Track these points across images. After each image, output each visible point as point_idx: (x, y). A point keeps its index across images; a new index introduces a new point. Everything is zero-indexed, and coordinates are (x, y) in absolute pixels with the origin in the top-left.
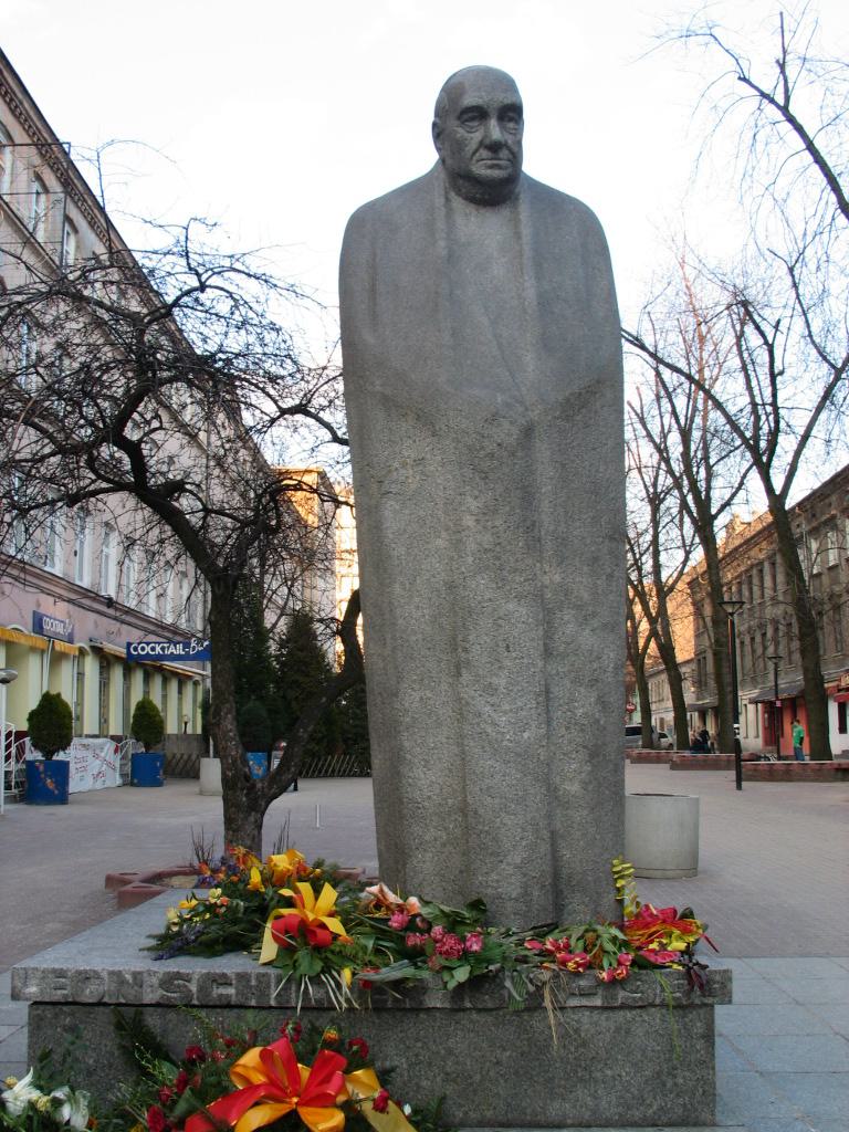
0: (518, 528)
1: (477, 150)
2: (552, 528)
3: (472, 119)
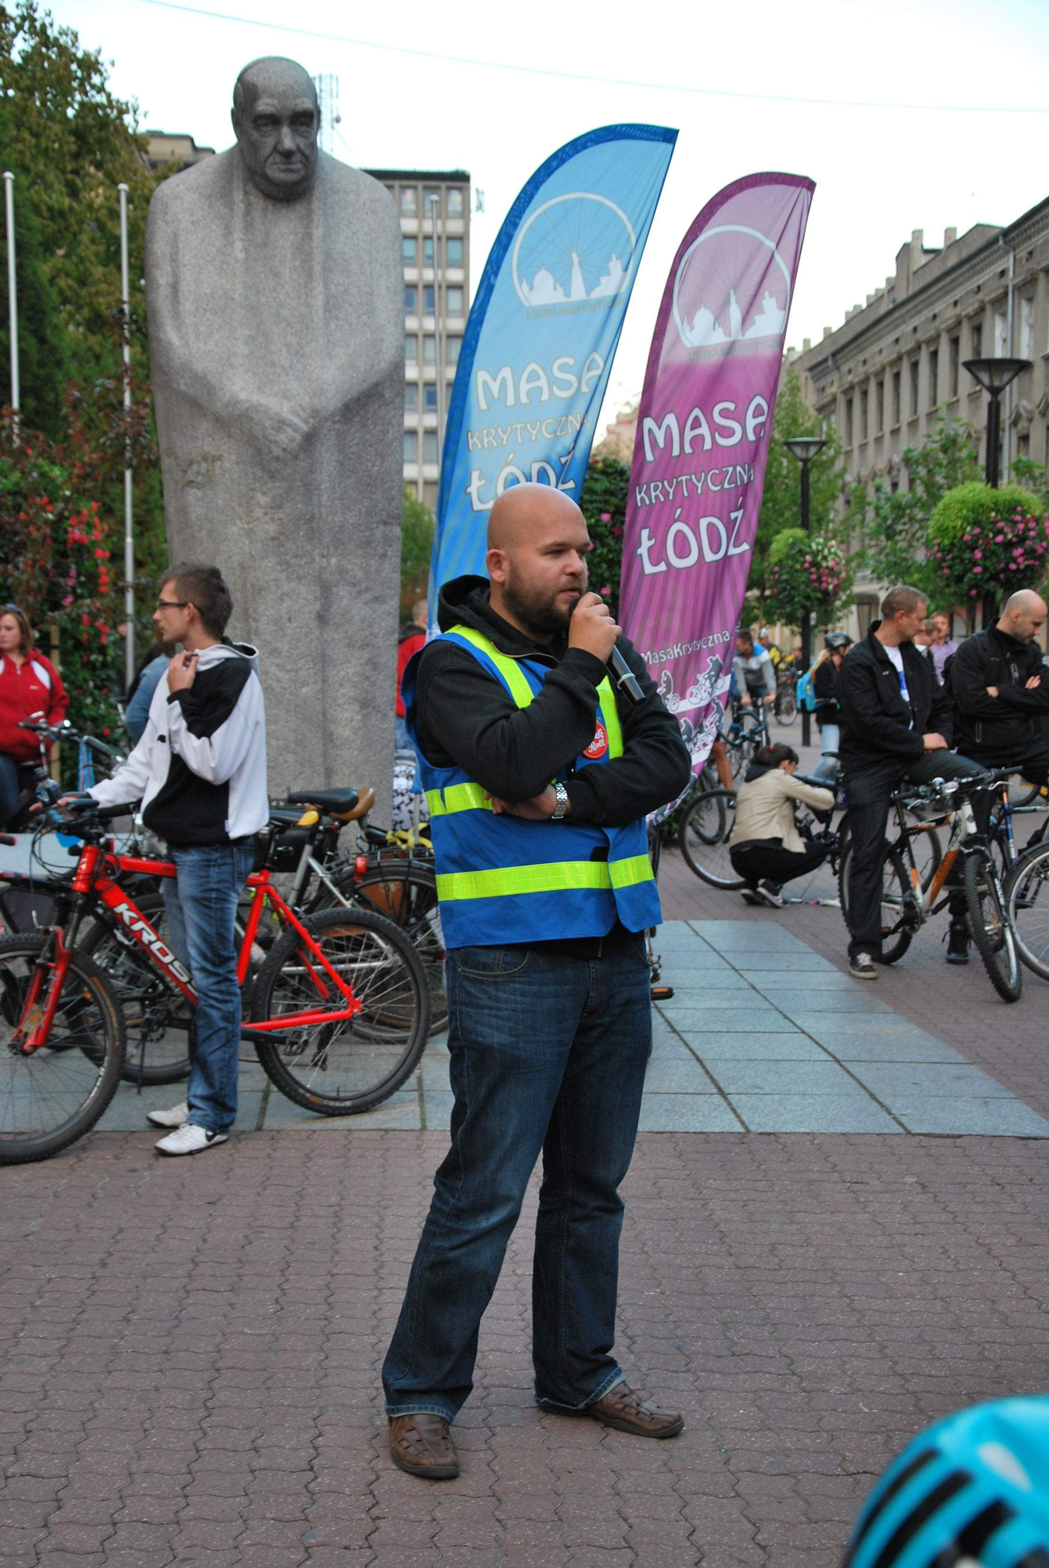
0: (299, 519)
1: (271, 155)
3: (266, 125)
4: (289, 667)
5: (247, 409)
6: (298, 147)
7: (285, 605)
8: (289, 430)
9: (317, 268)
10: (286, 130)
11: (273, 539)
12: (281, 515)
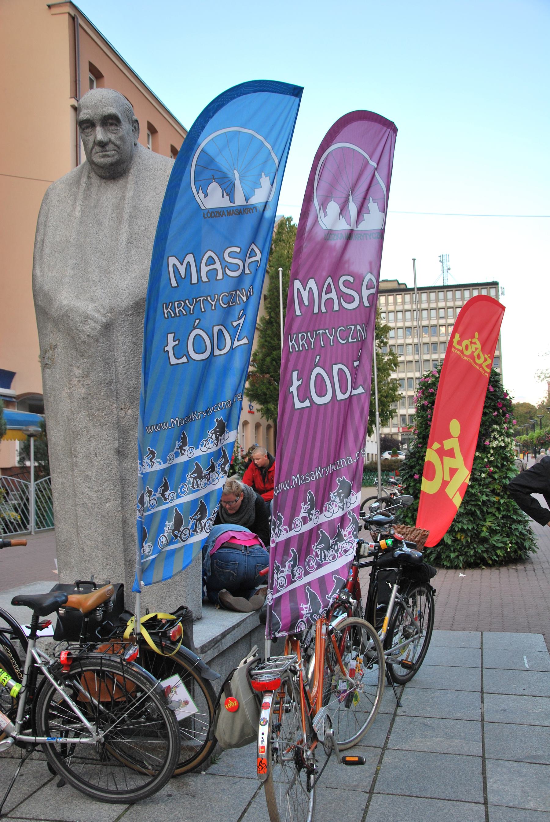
0: (101, 384)
1: (93, 148)
2: (125, 382)
4: (96, 489)
5: (67, 311)
6: (110, 141)
7: (92, 445)
8: (92, 322)
9: (126, 216)
10: (99, 129)
11: (83, 399)
12: (88, 382)
